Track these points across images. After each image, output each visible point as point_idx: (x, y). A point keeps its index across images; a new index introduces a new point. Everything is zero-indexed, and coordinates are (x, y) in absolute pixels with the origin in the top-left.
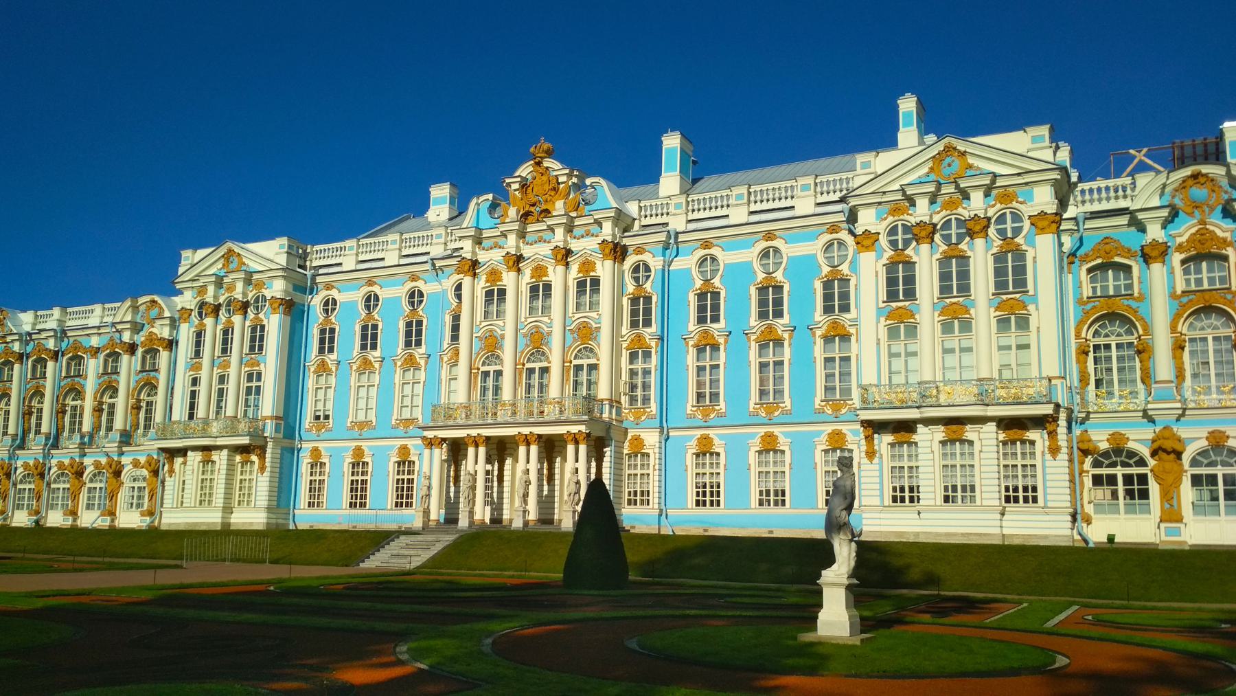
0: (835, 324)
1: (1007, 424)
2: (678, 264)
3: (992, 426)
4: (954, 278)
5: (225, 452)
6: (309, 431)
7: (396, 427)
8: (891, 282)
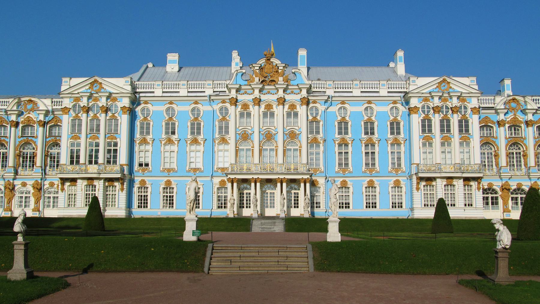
0: (396, 139)
1: (466, 179)
2: (331, 109)
3: (462, 180)
4: (445, 126)
5: (102, 181)
6: (138, 171)
7: (189, 171)
8: (423, 126)
